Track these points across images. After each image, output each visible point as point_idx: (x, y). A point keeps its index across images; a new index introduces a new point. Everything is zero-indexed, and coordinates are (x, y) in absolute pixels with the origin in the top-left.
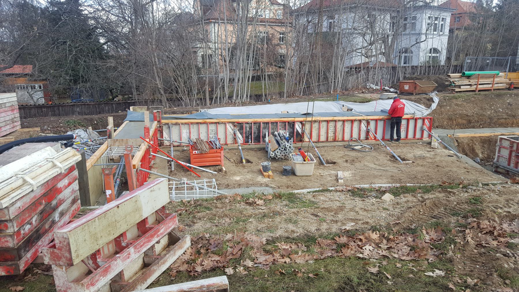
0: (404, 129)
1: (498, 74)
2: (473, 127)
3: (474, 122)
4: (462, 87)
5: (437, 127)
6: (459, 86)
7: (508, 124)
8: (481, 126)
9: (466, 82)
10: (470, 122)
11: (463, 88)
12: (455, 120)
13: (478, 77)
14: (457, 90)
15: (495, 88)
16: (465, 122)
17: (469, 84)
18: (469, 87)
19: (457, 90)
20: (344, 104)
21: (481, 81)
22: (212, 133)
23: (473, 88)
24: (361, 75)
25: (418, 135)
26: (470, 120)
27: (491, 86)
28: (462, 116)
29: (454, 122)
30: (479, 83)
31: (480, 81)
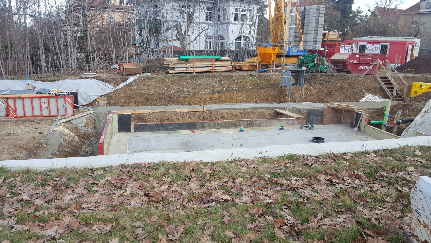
0: (46, 107)
1: (220, 59)
2: (150, 105)
3: (152, 100)
5: (114, 105)
6: (173, 69)
7: (185, 102)
8: (159, 104)
9: (183, 64)
10: (148, 100)
11: (177, 71)
12: (133, 99)
13: (194, 61)
14: (171, 71)
15: (214, 70)
16: (143, 100)
17: (186, 66)
18: (185, 69)
19: (171, 71)
20: (30, 83)
21: (198, 64)
22: (44, 105)
23: (190, 70)
24: (143, 57)
25: (62, 112)
26: (148, 98)
27: (211, 68)
28: (141, 95)
29: (132, 100)
30: (196, 66)
31: (214, 63)
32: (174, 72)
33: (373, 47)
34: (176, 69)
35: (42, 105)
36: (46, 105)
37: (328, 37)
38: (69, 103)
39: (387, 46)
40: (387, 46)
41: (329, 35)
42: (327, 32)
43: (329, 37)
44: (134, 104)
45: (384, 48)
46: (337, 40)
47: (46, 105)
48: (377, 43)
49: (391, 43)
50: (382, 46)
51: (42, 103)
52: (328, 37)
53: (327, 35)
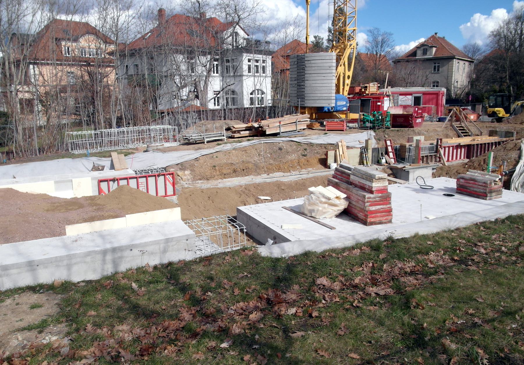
32: (240, 136)
33: (406, 98)
34: (242, 132)
35: (140, 186)
36: (144, 185)
37: (369, 89)
38: (169, 181)
39: (420, 97)
40: (420, 97)
41: (371, 88)
42: (368, 85)
43: (371, 90)
44: (220, 177)
45: (417, 101)
46: (376, 92)
47: (144, 185)
48: (410, 94)
49: (424, 94)
50: (415, 97)
51: (139, 184)
52: (369, 89)
53: (368, 87)
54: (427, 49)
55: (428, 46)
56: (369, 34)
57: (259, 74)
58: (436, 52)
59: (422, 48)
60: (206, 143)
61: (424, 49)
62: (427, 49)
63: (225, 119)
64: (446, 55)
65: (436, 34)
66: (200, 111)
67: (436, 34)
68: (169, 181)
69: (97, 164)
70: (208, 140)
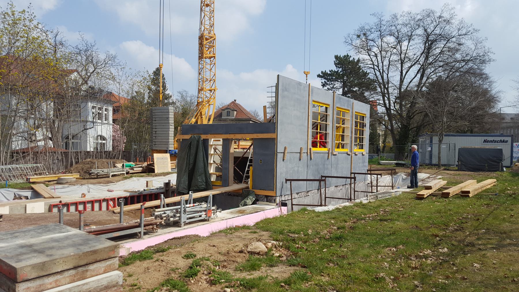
4: (135, 169)
54: (229, 112)
55: (231, 109)
56: (179, 95)
57: (107, 122)
58: (236, 114)
59: (226, 111)
60: (111, 177)
61: (227, 111)
62: (229, 112)
63: (106, 159)
64: (244, 117)
65: (235, 100)
66: (78, 152)
67: (235, 100)
68: (111, 206)
69: (18, 194)
70: (113, 174)
